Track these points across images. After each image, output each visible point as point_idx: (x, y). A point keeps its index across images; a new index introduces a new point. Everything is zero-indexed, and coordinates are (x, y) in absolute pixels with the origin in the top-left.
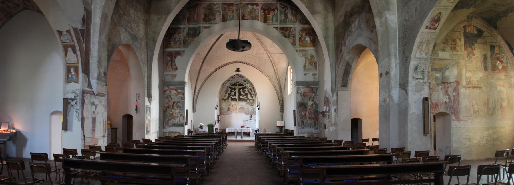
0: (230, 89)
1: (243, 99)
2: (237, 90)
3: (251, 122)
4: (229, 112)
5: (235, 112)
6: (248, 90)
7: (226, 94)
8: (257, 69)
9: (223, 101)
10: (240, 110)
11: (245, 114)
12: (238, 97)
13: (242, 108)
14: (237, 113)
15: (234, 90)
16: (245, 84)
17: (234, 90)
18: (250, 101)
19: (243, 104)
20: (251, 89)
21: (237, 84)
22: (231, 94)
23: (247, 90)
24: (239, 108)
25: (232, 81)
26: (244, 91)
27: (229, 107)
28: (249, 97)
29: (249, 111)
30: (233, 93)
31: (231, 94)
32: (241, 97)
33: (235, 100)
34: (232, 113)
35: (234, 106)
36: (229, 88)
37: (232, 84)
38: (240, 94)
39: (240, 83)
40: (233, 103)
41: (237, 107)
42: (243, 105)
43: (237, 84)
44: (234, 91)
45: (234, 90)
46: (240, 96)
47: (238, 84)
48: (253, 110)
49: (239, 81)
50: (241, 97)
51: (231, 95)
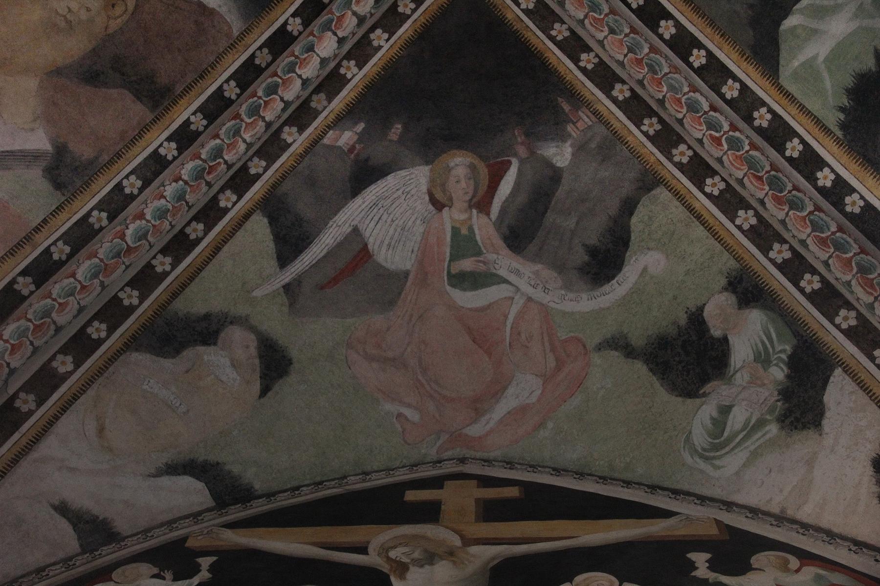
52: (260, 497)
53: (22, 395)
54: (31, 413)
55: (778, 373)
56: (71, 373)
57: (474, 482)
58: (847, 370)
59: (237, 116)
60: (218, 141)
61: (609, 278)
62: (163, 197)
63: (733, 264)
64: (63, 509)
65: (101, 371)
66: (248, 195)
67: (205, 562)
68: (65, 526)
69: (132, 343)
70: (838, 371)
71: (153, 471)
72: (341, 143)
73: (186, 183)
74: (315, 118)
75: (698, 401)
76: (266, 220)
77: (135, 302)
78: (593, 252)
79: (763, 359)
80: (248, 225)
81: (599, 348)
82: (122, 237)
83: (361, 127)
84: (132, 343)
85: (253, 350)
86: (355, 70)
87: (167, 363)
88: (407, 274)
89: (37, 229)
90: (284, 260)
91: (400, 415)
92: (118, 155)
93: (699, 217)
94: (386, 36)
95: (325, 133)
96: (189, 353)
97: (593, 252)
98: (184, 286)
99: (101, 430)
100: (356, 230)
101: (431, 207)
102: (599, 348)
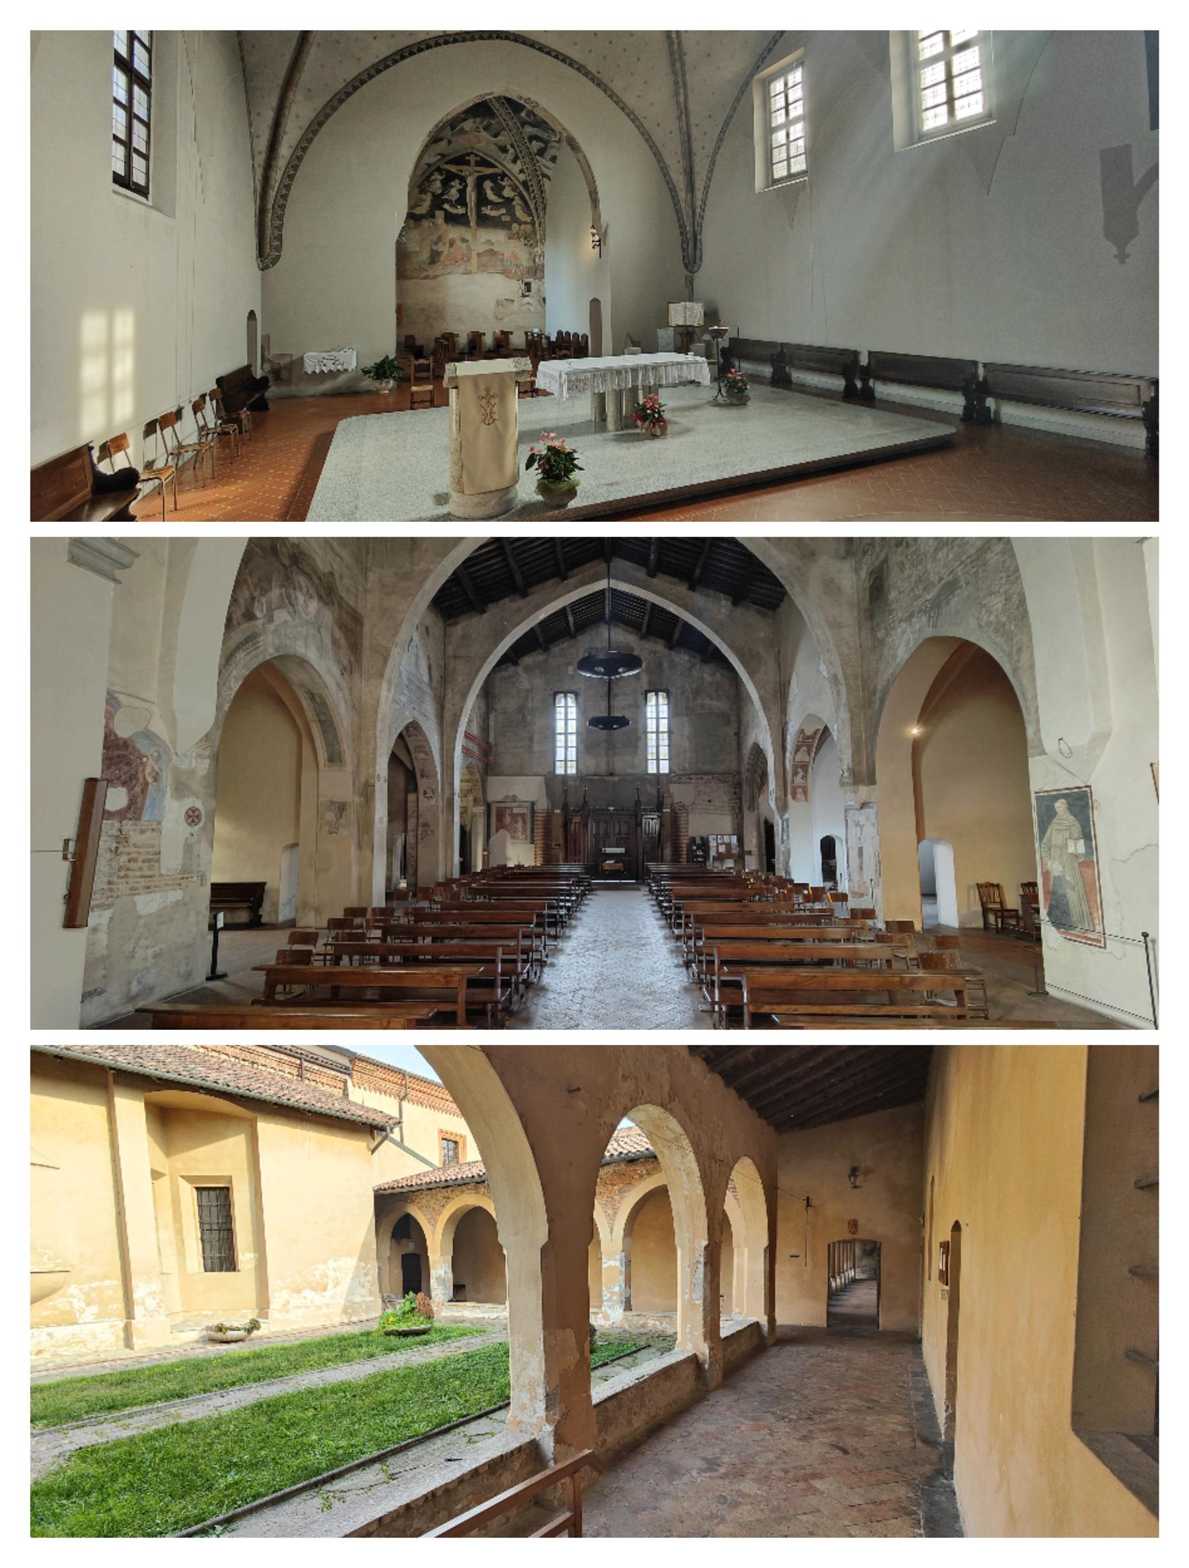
0: (440, 177)
2: (470, 181)
4: (437, 269)
5: (461, 269)
6: (514, 188)
10: (484, 259)
11: (503, 277)
13: (492, 253)
14: (468, 273)
15: (457, 181)
16: (505, 163)
17: (456, 183)
19: (497, 238)
20: (525, 184)
21: (467, 158)
22: (446, 197)
24: (479, 255)
25: (450, 142)
26: (498, 190)
27: (435, 247)
28: (519, 213)
30: (454, 194)
31: (446, 197)
32: (487, 211)
33: (461, 220)
35: (458, 242)
36: (436, 173)
37: (448, 159)
38: (482, 200)
39: (482, 158)
40: (454, 232)
41: (468, 247)
43: (467, 158)
44: (459, 187)
45: (457, 181)
47: (472, 159)
48: (534, 260)
49: (477, 146)
50: (487, 211)
51: (447, 201)
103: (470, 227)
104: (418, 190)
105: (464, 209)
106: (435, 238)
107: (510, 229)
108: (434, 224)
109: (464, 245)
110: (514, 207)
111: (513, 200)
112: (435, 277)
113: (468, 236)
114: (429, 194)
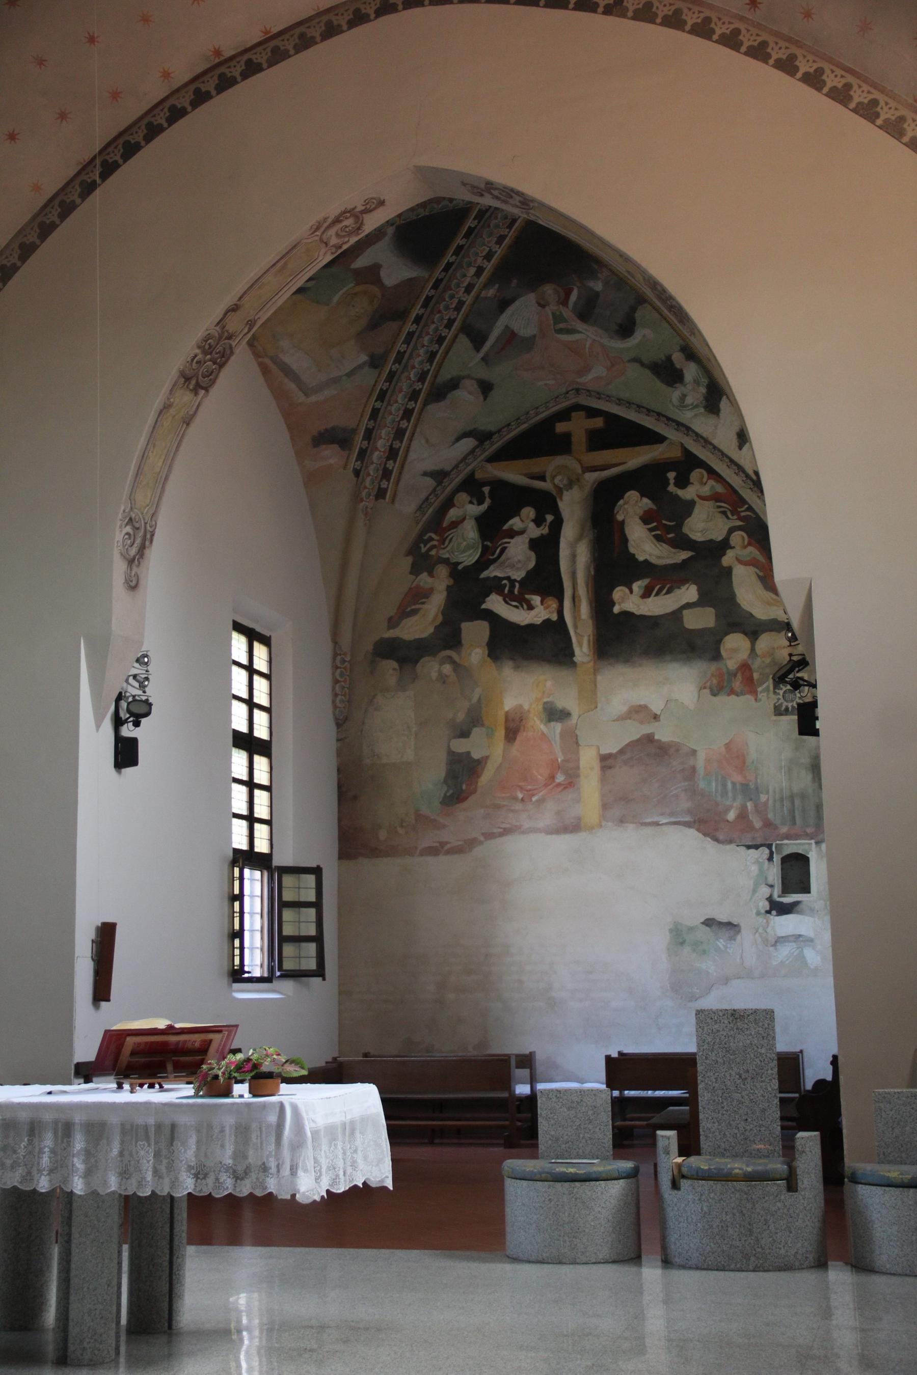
0: (475, 510)
1: (653, 622)
3: (785, 952)
5: (547, 819)
7: (424, 579)
8: (748, 40)
9: (389, 667)
10: (625, 775)
12: (585, 609)
14: (573, 827)
15: (529, 512)
16: (686, 416)
18: (765, 642)
21: (561, 427)
22: (492, 572)
23: (715, 498)
24: (607, 761)
25: (486, 388)
27: (460, 746)
29: (748, 791)
31: (492, 572)
34: (506, 832)
35: (537, 724)
36: (463, 497)
37: (497, 444)
39: (611, 419)
41: (572, 741)
42: (656, 706)
43: (561, 427)
44: (535, 532)
45: (529, 512)
46: (618, 593)
49: (587, 379)
51: (496, 586)
52: (495, 433)
53: (394, 442)
54: (400, 447)
55: (703, 390)
56: (408, 426)
57: (582, 414)
58: (728, 398)
59: (439, 312)
60: (435, 325)
61: (630, 336)
62: (420, 356)
63: (681, 342)
64: (425, 474)
65: (418, 420)
66: (454, 328)
67: (486, 490)
68: (428, 479)
69: (426, 403)
70: (725, 397)
71: (451, 444)
72: (489, 295)
73: (427, 346)
74: (474, 287)
75: (674, 389)
76: (465, 336)
77: (421, 387)
78: (620, 326)
79: (697, 382)
80: (458, 340)
81: (629, 361)
82: (410, 379)
83: (497, 286)
84: (426, 404)
85: (476, 386)
86: (487, 263)
87: (442, 404)
88: (535, 336)
89: (374, 385)
90: (478, 349)
91: (546, 384)
92: (394, 343)
93: (665, 319)
94: (498, 246)
95: (480, 293)
96: (449, 396)
97: (620, 326)
98: (438, 371)
99: (427, 441)
100: (507, 327)
101: (539, 308)
102: (629, 361)
103: (573, 664)
104: (410, 559)
105: (553, 604)
106: (461, 716)
107: (716, 656)
108: (456, 665)
109: (558, 727)
110: (728, 572)
111: (724, 545)
112: (465, 847)
113: (568, 700)
114: (442, 571)
